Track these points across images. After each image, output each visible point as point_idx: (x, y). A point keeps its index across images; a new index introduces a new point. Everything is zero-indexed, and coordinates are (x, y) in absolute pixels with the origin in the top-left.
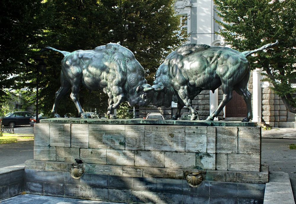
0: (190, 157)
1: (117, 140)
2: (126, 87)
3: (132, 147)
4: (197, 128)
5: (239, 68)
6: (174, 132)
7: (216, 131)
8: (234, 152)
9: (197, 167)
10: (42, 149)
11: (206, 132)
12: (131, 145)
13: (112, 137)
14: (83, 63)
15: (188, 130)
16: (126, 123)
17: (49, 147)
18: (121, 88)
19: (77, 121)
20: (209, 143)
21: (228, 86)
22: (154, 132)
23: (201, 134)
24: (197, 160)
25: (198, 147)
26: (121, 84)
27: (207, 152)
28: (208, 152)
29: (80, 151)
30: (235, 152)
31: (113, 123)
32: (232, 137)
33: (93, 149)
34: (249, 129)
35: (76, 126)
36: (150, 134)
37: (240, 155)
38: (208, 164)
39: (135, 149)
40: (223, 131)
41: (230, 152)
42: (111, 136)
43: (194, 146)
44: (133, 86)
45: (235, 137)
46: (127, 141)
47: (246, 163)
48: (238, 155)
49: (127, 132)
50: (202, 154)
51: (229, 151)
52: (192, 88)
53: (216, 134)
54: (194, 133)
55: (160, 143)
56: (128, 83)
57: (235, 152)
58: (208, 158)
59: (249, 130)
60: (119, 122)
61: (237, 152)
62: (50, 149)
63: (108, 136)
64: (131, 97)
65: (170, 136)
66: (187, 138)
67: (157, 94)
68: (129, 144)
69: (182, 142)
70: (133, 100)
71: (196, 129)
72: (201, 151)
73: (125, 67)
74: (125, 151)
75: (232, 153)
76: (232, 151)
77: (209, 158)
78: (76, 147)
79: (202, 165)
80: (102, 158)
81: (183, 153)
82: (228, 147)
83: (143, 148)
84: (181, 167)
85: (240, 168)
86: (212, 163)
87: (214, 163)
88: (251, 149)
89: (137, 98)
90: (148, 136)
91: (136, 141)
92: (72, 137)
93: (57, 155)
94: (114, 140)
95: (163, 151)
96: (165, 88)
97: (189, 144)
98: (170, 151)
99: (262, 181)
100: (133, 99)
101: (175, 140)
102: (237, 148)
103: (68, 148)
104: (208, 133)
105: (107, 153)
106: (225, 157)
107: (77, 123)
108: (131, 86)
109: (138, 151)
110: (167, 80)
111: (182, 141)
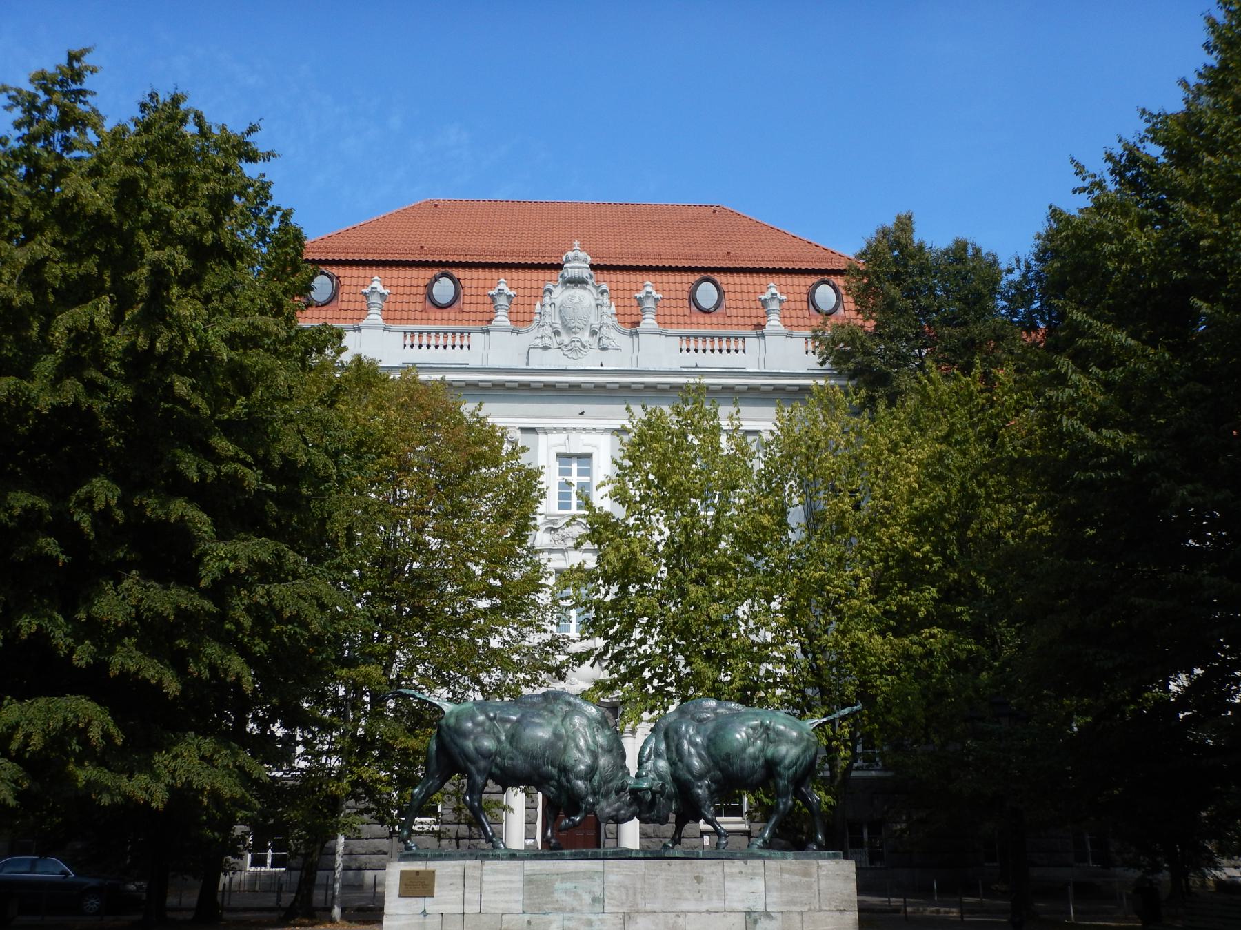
5: (804, 751)
41: (805, 908)
52: (713, 787)
54: (741, 872)
55: (677, 896)
64: (603, 803)
67: (649, 797)
70: (608, 810)
73: (595, 742)
75: (810, 910)
83: (641, 907)
106: (797, 918)
108: (606, 781)
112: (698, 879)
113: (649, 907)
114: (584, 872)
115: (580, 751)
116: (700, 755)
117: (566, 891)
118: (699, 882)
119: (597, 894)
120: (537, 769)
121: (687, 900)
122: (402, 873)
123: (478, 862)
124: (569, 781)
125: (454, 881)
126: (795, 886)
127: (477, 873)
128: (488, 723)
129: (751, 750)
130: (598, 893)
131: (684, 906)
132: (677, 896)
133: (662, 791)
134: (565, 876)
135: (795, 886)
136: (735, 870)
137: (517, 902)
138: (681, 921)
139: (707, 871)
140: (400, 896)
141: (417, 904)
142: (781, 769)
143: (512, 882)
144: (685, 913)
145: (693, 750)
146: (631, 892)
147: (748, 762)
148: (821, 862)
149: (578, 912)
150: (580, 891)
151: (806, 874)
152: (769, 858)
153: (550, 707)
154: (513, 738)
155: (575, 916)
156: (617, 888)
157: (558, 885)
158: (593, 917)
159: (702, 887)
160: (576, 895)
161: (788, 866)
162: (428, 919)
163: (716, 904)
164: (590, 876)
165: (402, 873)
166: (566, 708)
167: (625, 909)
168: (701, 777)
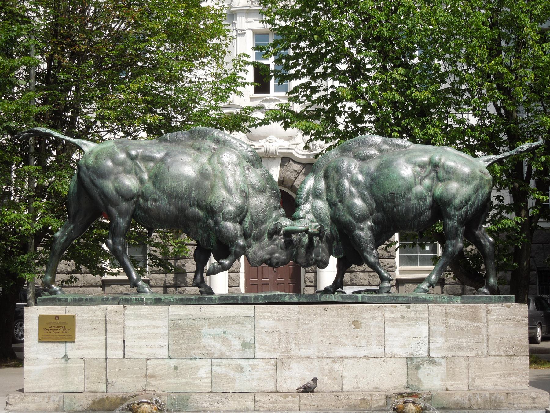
2: (247, 224)
3: (270, 351)
4: (409, 308)
5: (477, 190)
6: (362, 317)
7: (446, 313)
10: (48, 366)
11: (427, 315)
12: (268, 348)
13: (224, 332)
14: (140, 169)
15: (391, 312)
16: (253, 302)
17: (66, 361)
18: (238, 226)
19: (136, 299)
20: (433, 337)
22: (319, 319)
23: (417, 320)
24: (410, 372)
25: (411, 346)
26: (238, 219)
27: (429, 356)
28: (432, 355)
29: (147, 365)
30: (483, 353)
32: (475, 324)
33: (180, 361)
34: (508, 308)
35: (137, 309)
37: (492, 358)
38: (432, 380)
39: (278, 357)
40: (459, 312)
41: (472, 354)
42: (222, 330)
43: (402, 344)
44: (263, 223)
45: (482, 324)
46: (259, 339)
48: (489, 358)
49: (260, 319)
50: (419, 360)
51: (471, 351)
54: (403, 317)
56: (251, 215)
57: (483, 353)
58: (431, 367)
59: (508, 309)
60: (237, 300)
61: (485, 353)
62: (68, 365)
63: (215, 329)
65: (354, 326)
67: (306, 240)
68: (263, 345)
69: (379, 336)
70: (261, 253)
71: (407, 310)
72: (419, 352)
75: (477, 355)
76: (476, 352)
77: (434, 368)
78: (137, 356)
80: (202, 378)
83: (295, 353)
84: (376, 388)
85: (492, 383)
86: (439, 376)
88: (513, 346)
90: (306, 327)
91: (280, 339)
92: (126, 334)
93: (88, 379)
94: (229, 339)
96: (322, 227)
98: (354, 357)
100: (260, 251)
101: (363, 333)
102: (485, 345)
103: (116, 361)
105: (214, 368)
106: (464, 363)
108: (256, 223)
109: (285, 360)
110: (324, 211)
111: (379, 334)
112: (357, 324)
113: (303, 353)
114: (233, 317)
115: (229, 191)
116: (362, 196)
117: (214, 337)
118: (357, 328)
119: (248, 340)
120: (182, 210)
121: (346, 345)
122: (41, 317)
123: (121, 307)
124: (216, 223)
125: (95, 326)
126: (462, 331)
127: (120, 318)
128: (129, 162)
130: (249, 337)
131: (341, 352)
132: (333, 341)
133: (320, 234)
134: (213, 321)
135: (462, 331)
136: (397, 315)
137: (162, 347)
138: (337, 366)
139: (365, 316)
140: (40, 341)
141: (59, 349)
142: (450, 210)
143: (156, 327)
144: (342, 358)
145: (353, 190)
146: (283, 338)
147: (415, 202)
148: (492, 306)
149: (227, 358)
150: (229, 337)
151: (474, 318)
153: (197, 144)
154: (156, 178)
155: (225, 361)
156: (269, 333)
157: (205, 330)
158: (244, 363)
159: (360, 332)
160: (225, 340)
162: (70, 364)
163: (377, 350)
164: (239, 320)
165: (42, 318)
166: (213, 145)
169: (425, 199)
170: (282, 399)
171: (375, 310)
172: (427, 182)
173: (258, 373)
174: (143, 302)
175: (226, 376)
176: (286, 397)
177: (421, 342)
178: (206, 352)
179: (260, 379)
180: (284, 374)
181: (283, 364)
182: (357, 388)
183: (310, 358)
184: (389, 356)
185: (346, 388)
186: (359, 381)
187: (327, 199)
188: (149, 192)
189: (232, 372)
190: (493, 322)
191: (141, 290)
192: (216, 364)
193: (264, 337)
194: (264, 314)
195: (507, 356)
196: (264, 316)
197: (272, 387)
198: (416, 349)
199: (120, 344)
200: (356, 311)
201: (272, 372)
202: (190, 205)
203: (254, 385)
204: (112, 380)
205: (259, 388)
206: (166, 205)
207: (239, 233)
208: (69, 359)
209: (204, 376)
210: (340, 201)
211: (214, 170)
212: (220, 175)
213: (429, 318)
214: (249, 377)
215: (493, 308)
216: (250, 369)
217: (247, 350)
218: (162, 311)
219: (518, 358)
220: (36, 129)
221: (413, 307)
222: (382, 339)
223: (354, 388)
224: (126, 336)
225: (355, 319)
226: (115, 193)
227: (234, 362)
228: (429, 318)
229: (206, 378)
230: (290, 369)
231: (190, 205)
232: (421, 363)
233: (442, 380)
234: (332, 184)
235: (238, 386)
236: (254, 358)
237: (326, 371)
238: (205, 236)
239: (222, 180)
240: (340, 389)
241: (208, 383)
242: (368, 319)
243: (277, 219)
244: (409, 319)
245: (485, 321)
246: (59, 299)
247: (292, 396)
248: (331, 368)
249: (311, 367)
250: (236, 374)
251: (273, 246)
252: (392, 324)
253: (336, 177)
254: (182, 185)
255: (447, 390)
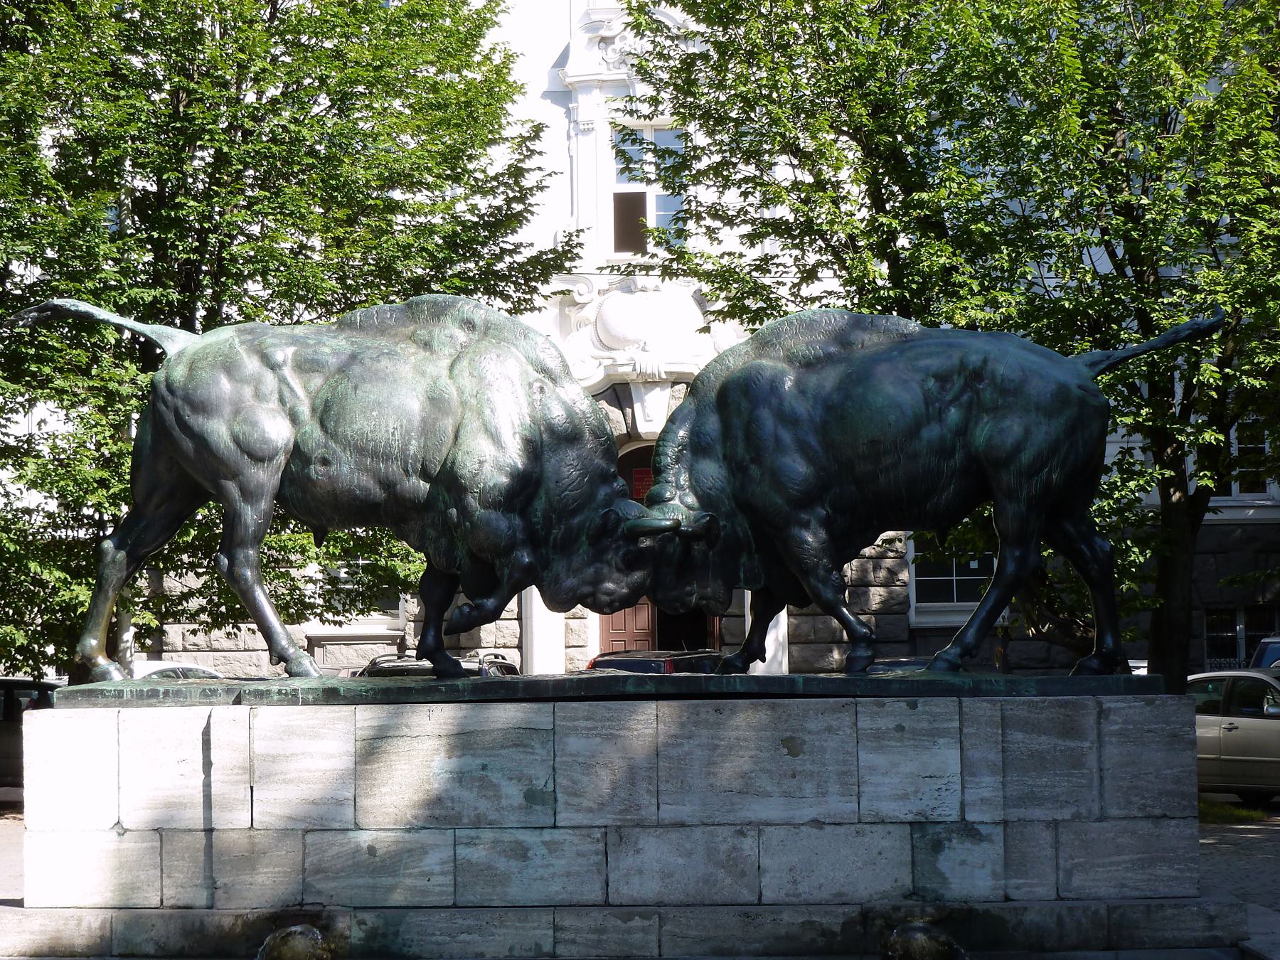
0: (885, 843)
1: (511, 779)
2: (539, 514)
4: (913, 706)
7: (1003, 718)
8: (1083, 811)
9: (914, 893)
11: (957, 724)
12: (586, 803)
13: (484, 767)
14: (292, 390)
18: (517, 521)
19: (280, 692)
20: (973, 775)
21: (1024, 509)
22: (704, 732)
23: (935, 734)
24: (920, 857)
25: (920, 795)
27: (963, 819)
28: (971, 817)
30: (1090, 812)
31: (483, 697)
32: (1072, 744)
34: (1148, 704)
36: (682, 744)
37: (1113, 822)
38: (971, 875)
39: (610, 823)
41: (1066, 814)
42: (479, 761)
43: (900, 792)
44: (574, 513)
45: (1087, 744)
47: (1139, 859)
48: (1104, 824)
49: (567, 735)
50: (939, 828)
51: (1062, 807)
53: (1003, 735)
54: (900, 728)
57: (1090, 812)
58: (968, 845)
59: (1148, 709)
61: (1096, 809)
64: (559, 567)
65: (785, 751)
66: (866, 757)
68: (575, 795)
69: (844, 773)
74: (556, 831)
75: (1077, 816)
76: (1074, 810)
77: (977, 848)
79: (945, 879)
80: (432, 874)
81: (853, 828)
82: (1058, 790)
83: (649, 813)
84: (840, 894)
86: (988, 869)
87: (999, 869)
89: (591, 570)
92: (257, 774)
93: (169, 877)
95: (750, 823)
97: (877, 785)
99: (1219, 933)
100: (568, 577)
101: (808, 767)
102: (1095, 792)
104: (965, 731)
106: (1046, 836)
107: (280, 703)
108: (563, 511)
109: (626, 832)
111: (844, 769)
112: (792, 746)
113: (669, 813)
116: (804, 449)
120: (388, 485)
121: (768, 795)
123: (243, 709)
129: (931, 432)
130: (541, 779)
138: (748, 844)
144: (761, 826)
145: (786, 436)
148: (1110, 702)
149: (492, 825)
150: (494, 777)
151: (1070, 730)
152: (975, 692)
153: (423, 333)
155: (488, 835)
158: (529, 837)
161: (1022, 713)
163: (840, 805)
166: (461, 336)
167: (608, 819)
168: (806, 500)
169: (951, 453)
170: (619, 922)
171: (834, 711)
172: (954, 414)
173: (563, 862)
174: (295, 696)
175: (490, 867)
176: (629, 918)
177: (944, 787)
178: (444, 813)
179: (568, 874)
180: (624, 862)
181: (621, 838)
182: (794, 895)
183: (683, 825)
184: (869, 820)
185: (768, 896)
186: (799, 879)
187: (725, 457)
188: (312, 444)
189: (503, 859)
190: (1114, 739)
191: (295, 669)
192: (465, 841)
193: (577, 776)
194: (576, 723)
195: (1148, 817)
196: (575, 728)
197: (595, 894)
198: (933, 803)
199: (242, 797)
200: (789, 715)
201: (594, 858)
202: (407, 472)
203: (556, 890)
204: (226, 880)
205: (564, 896)
206: (352, 472)
207: (520, 536)
208: (126, 831)
209: (437, 869)
210: (753, 461)
211: (461, 392)
212: (473, 401)
213: (961, 730)
214: (541, 871)
215: (1113, 705)
216: (545, 851)
217: (538, 808)
218: (339, 719)
219: (1174, 822)
220: (57, 301)
221: (925, 704)
222: (853, 783)
223: (787, 895)
224: (256, 779)
225: (788, 734)
226: (232, 445)
227: (507, 837)
228: (961, 730)
229: (442, 874)
230: (638, 851)
231: (407, 472)
232: (944, 835)
233: (995, 875)
234: (736, 421)
235: (516, 892)
236: (555, 827)
237: (723, 857)
238: (443, 541)
239: (480, 413)
240: (754, 899)
241: (447, 886)
242: (818, 733)
243: (608, 502)
244: (915, 733)
245: (1093, 736)
246: (102, 693)
247: (642, 916)
248: (735, 848)
249: (688, 846)
250: (513, 863)
251: (598, 565)
252: (875, 744)
253: (744, 404)
254: (387, 426)
255: (1007, 899)
